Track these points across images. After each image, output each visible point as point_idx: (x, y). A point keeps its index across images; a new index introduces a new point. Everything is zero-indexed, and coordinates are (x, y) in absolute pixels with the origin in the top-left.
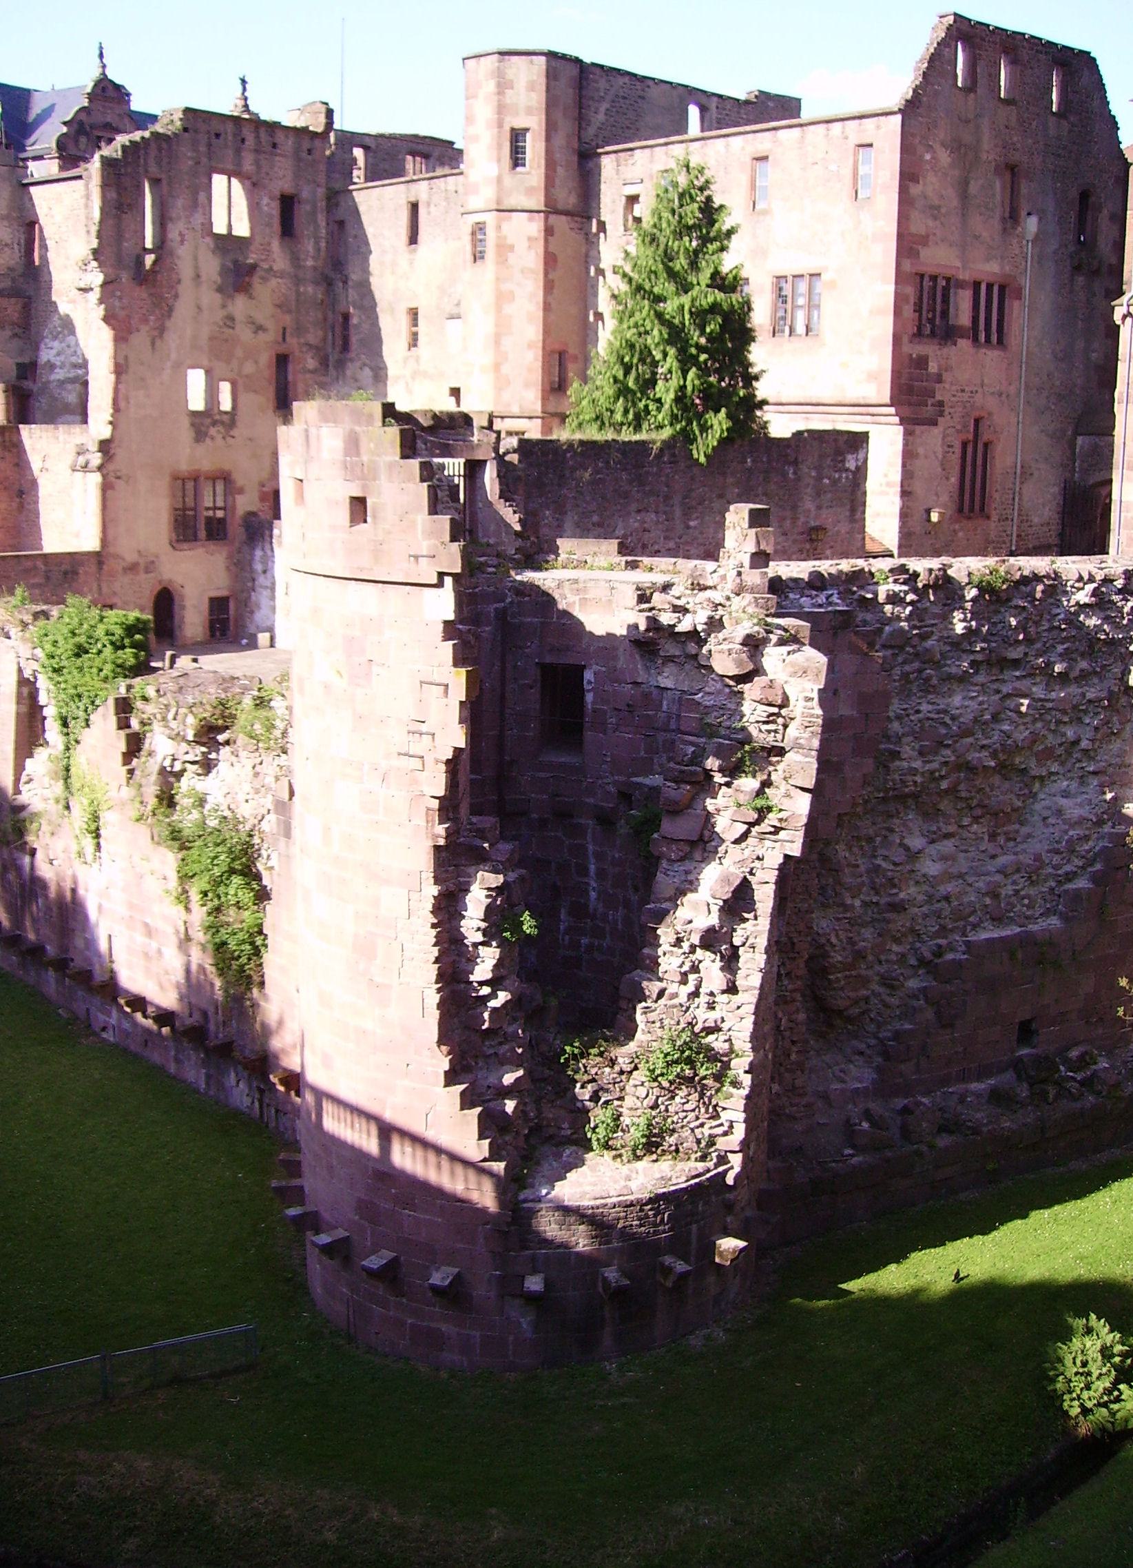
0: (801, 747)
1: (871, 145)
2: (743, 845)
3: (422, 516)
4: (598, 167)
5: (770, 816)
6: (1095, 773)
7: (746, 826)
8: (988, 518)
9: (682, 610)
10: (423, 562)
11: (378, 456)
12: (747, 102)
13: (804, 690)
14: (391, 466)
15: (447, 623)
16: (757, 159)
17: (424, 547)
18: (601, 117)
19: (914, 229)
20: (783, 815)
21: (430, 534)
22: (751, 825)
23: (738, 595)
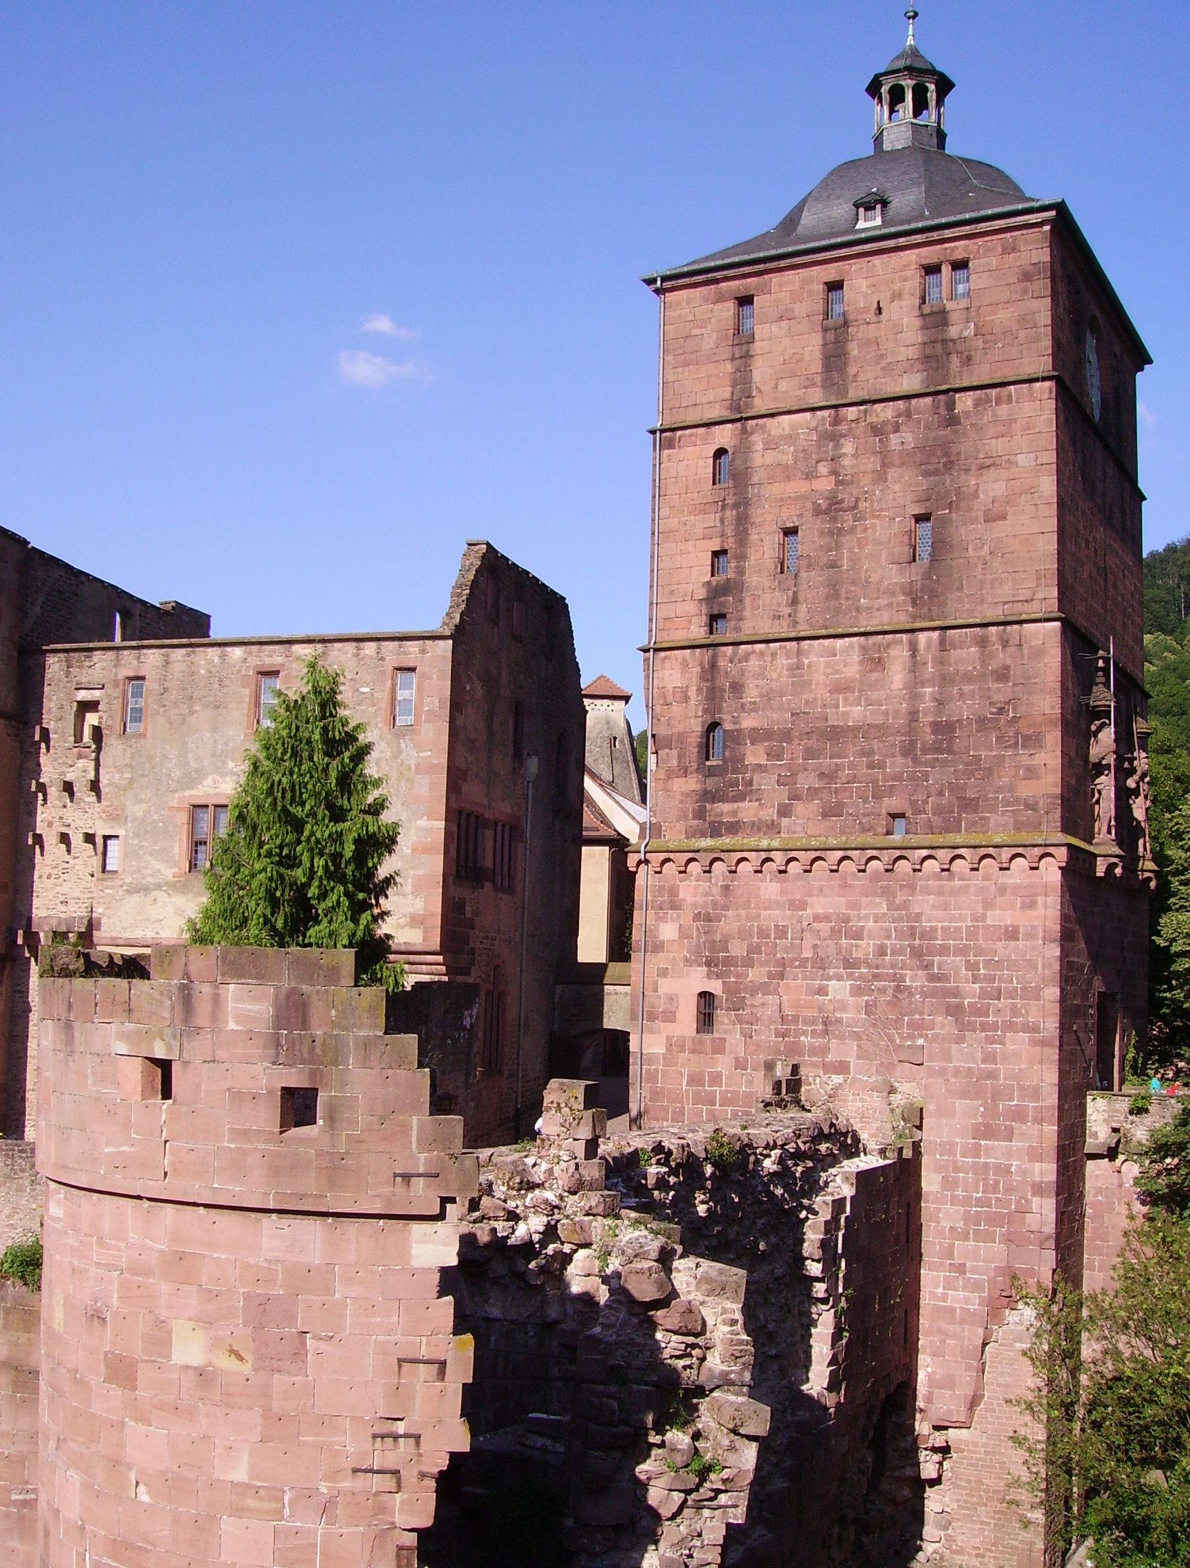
0: (732, 1383)
1: (413, 669)
2: (679, 1520)
3: (419, 1120)
4: (42, 668)
5: (712, 1476)
6: (776, 1357)
7: (683, 1495)
8: (501, 1073)
9: (513, 1217)
10: (419, 1184)
11: (347, 1029)
12: (167, 613)
13: (724, 1311)
14: (366, 1045)
15: (445, 1271)
16: (263, 673)
17: (421, 1162)
18: (37, 610)
19: (457, 764)
20: (726, 1474)
21: (427, 1143)
22: (688, 1492)
23: (574, 1193)
